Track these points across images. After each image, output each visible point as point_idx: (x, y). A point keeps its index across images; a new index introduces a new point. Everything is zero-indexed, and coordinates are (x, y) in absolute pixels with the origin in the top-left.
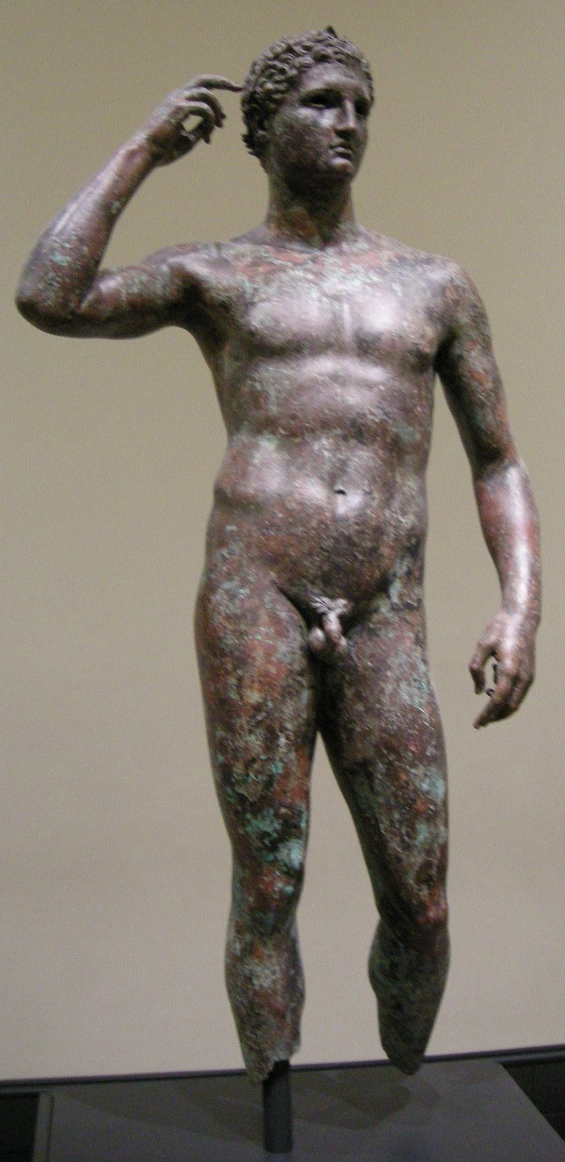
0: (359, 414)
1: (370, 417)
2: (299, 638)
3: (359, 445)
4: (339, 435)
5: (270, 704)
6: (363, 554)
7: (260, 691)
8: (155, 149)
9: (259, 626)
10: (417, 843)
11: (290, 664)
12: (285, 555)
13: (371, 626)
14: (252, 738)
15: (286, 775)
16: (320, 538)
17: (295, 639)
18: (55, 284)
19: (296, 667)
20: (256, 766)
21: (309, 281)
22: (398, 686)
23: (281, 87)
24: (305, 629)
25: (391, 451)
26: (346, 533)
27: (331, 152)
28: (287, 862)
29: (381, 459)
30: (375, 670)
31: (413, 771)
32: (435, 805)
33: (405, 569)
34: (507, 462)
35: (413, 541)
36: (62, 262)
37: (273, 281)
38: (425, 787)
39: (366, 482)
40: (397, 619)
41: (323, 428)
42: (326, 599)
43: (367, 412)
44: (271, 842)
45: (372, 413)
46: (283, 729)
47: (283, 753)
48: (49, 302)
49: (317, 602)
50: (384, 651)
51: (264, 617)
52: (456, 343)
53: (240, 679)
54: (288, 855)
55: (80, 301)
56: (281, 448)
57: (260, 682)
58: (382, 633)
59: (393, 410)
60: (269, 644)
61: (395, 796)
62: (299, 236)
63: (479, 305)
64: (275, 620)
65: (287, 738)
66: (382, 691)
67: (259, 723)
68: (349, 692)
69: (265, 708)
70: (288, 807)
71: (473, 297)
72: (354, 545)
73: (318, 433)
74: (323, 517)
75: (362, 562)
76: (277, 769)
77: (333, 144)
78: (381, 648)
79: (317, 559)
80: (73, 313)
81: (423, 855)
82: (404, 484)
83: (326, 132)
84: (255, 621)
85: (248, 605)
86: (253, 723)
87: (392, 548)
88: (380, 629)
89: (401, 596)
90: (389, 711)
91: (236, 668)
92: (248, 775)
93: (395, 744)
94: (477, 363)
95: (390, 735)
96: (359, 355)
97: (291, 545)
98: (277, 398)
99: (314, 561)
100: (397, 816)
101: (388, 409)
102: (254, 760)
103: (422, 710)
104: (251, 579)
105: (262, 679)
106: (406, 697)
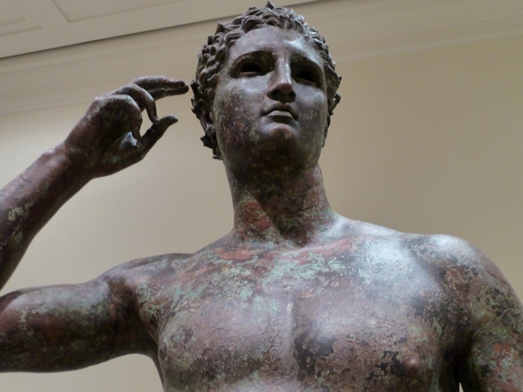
21: (244, 278)
27: (264, 119)
52: (475, 349)
62: (252, 230)
63: (503, 290)
71: (491, 280)
77: (266, 109)
83: (259, 99)
96: (301, 378)
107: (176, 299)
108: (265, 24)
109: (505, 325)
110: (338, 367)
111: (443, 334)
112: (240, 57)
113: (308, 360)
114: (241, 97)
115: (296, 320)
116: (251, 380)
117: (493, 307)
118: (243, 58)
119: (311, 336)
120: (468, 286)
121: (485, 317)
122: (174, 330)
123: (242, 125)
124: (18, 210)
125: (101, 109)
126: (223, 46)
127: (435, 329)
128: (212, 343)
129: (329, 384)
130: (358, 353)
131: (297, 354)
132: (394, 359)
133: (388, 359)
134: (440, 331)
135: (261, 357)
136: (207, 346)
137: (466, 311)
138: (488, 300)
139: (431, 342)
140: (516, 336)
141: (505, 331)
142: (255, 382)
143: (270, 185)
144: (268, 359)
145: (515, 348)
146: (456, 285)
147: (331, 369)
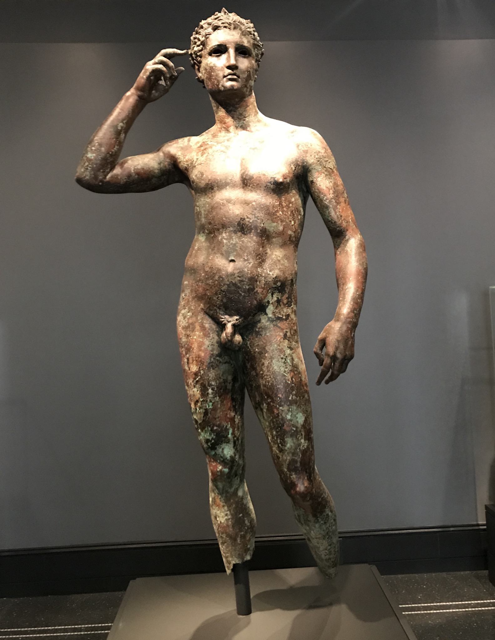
0: (241, 219)
1: (247, 220)
2: (216, 338)
3: (243, 235)
4: (232, 230)
5: (202, 372)
6: (244, 292)
7: (197, 365)
8: (139, 93)
9: (195, 332)
10: (286, 448)
11: (211, 351)
12: (205, 294)
13: (257, 330)
14: (195, 390)
15: (214, 409)
16: (220, 285)
17: (213, 338)
18: (89, 168)
19: (215, 352)
20: (199, 404)
22: (272, 361)
23: (200, 48)
24: (220, 332)
25: (261, 237)
26: (234, 282)
27: (225, 79)
28: (222, 456)
29: (255, 242)
30: (260, 353)
31: (281, 408)
32: (297, 428)
33: (275, 299)
34: (347, 237)
35: (279, 284)
36: (91, 157)
37: (205, 153)
38: (289, 417)
39: (246, 254)
40: (272, 326)
41: (223, 228)
42: (227, 317)
43: (246, 217)
44: (211, 444)
45: (248, 218)
46: (210, 385)
47: (211, 398)
48: (87, 177)
49: (223, 318)
50: (264, 343)
51: (198, 327)
53: (188, 359)
54: (223, 452)
55: (106, 176)
56: (207, 239)
57: (196, 360)
58: (263, 333)
59: (261, 215)
60: (200, 341)
61: (273, 422)
62: (224, 128)
64: (203, 328)
65: (212, 389)
66: (263, 364)
67: (197, 381)
68: (248, 366)
69: (199, 374)
70: (218, 426)
72: (239, 288)
73: (221, 230)
74: (221, 274)
75: (244, 296)
76: (210, 406)
77: (226, 74)
78: (263, 342)
79: (220, 296)
80: (101, 181)
81: (291, 455)
82: (273, 254)
83: (222, 69)
84: (193, 330)
85: (190, 321)
86: (195, 382)
87: (264, 288)
88: (262, 331)
89: (274, 313)
90: (267, 375)
91: (186, 354)
92: (196, 409)
93: (271, 393)
94: (322, 184)
95: (267, 388)
96: (243, 187)
97: (207, 290)
98: (204, 214)
99: (219, 297)
100: (274, 433)
101: (257, 215)
102: (197, 401)
103: (286, 375)
104: (192, 308)
105: (197, 359)
106: (275, 368)
107: (195, 160)
108: (222, 28)
109: (321, 165)
110: (255, 183)
111: (295, 170)
112: (212, 47)
113: (245, 181)
114: (214, 68)
115: (241, 167)
116: (226, 189)
117: (317, 158)
118: (214, 47)
119: (247, 173)
120: (307, 151)
121: (313, 162)
122: (196, 173)
123: (216, 82)
124: (121, 124)
125: (150, 73)
126: (204, 38)
127: (292, 168)
128: (211, 177)
129: (252, 189)
130: (262, 178)
131: (242, 179)
132: (274, 180)
133: (272, 180)
134: (294, 169)
135: (229, 181)
136: (210, 178)
137: (305, 160)
138: (315, 156)
139: (289, 173)
140: (325, 169)
141: (320, 167)
142: (227, 190)
143: (230, 107)
144: (232, 182)
145: (324, 173)
146: (303, 151)
147: (253, 184)
